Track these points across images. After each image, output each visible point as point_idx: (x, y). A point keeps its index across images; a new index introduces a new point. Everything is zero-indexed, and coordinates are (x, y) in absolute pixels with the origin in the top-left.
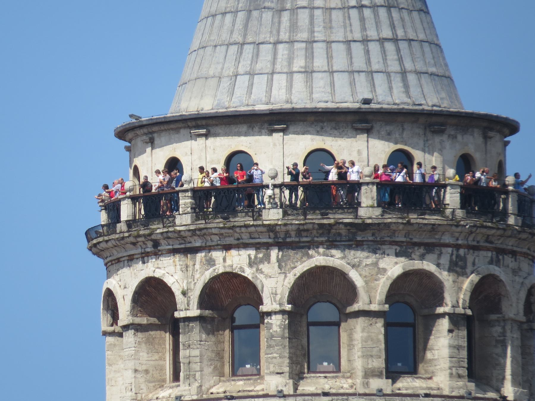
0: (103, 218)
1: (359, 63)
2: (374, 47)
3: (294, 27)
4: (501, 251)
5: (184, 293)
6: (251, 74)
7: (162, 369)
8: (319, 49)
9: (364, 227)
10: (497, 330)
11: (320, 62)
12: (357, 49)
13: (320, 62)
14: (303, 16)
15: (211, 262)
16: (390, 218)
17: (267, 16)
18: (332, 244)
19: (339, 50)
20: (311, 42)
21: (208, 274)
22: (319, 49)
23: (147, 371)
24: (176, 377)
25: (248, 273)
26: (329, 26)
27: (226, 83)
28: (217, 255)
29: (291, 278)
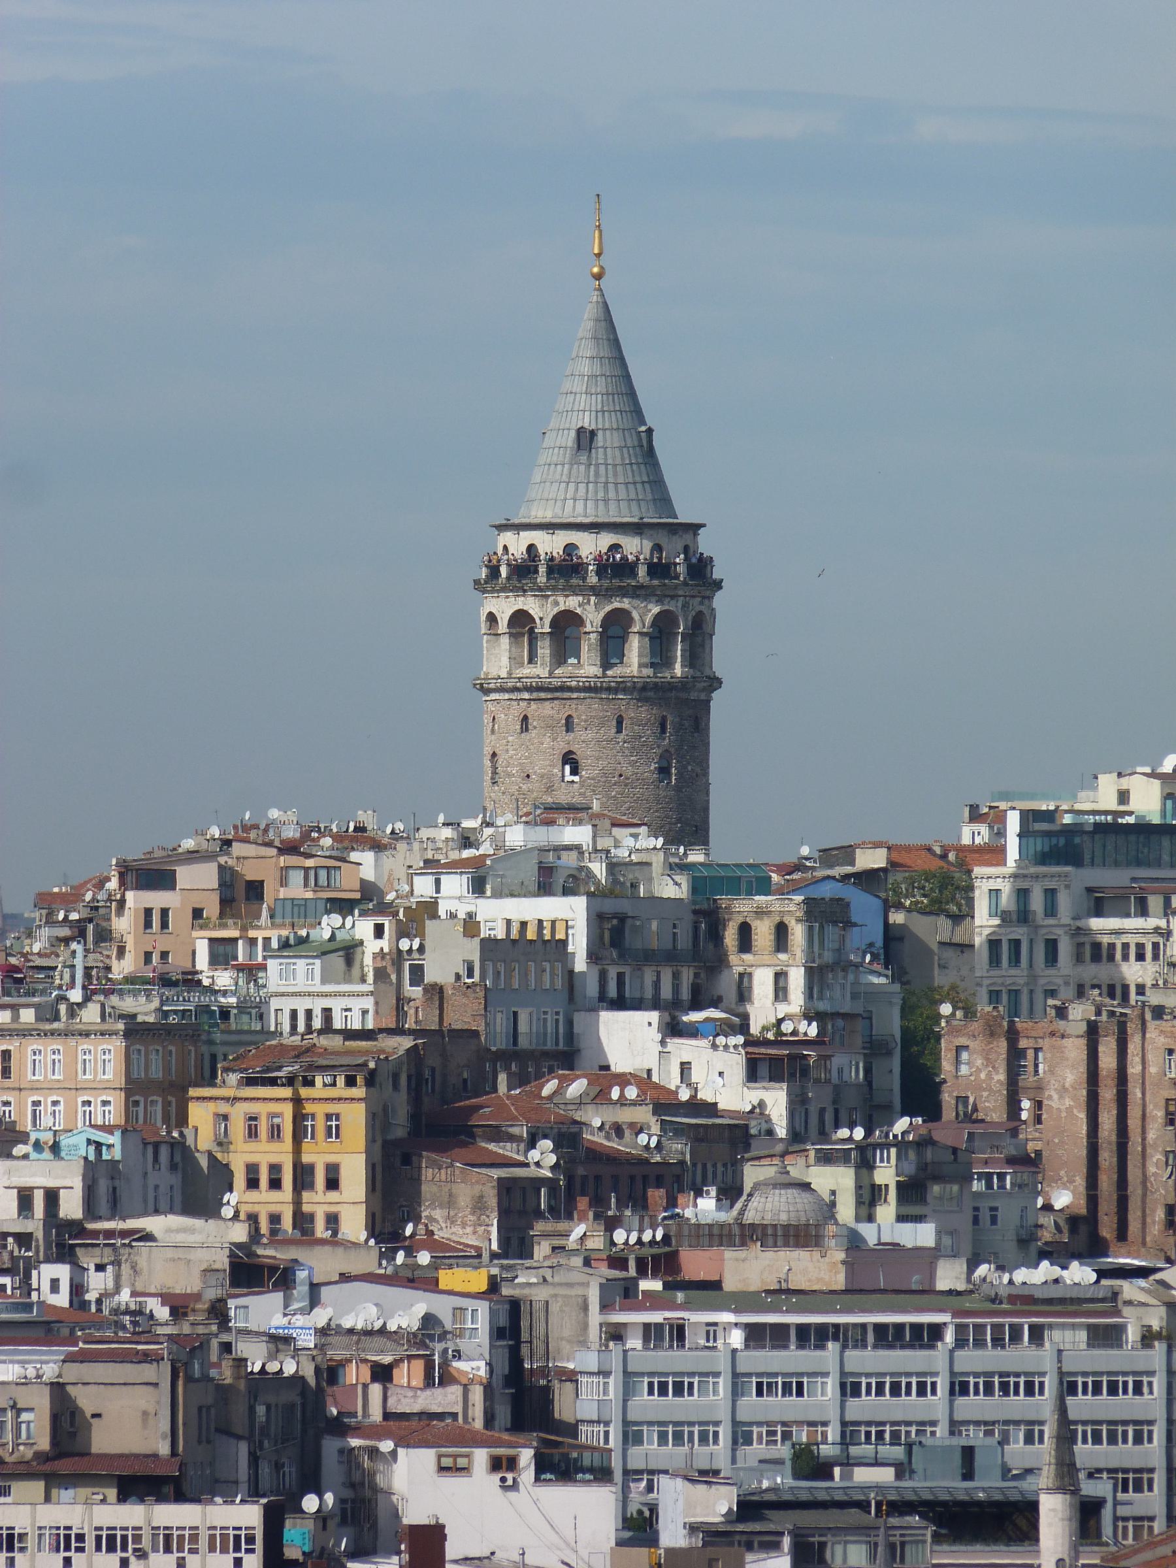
0: (484, 573)
1: (633, 496)
2: (639, 486)
3: (597, 474)
4: (704, 597)
5: (541, 619)
6: (575, 500)
7: (523, 657)
8: (611, 486)
9: (642, 587)
10: (699, 639)
11: (612, 495)
12: (631, 487)
13: (612, 495)
14: (602, 468)
15: (556, 603)
16: (656, 582)
17: (582, 468)
18: (624, 596)
19: (621, 487)
20: (606, 483)
21: (556, 610)
22: (611, 486)
23: (515, 659)
24: (530, 661)
25: (579, 611)
26: (615, 474)
27: (559, 504)
28: (561, 599)
29: (602, 614)
